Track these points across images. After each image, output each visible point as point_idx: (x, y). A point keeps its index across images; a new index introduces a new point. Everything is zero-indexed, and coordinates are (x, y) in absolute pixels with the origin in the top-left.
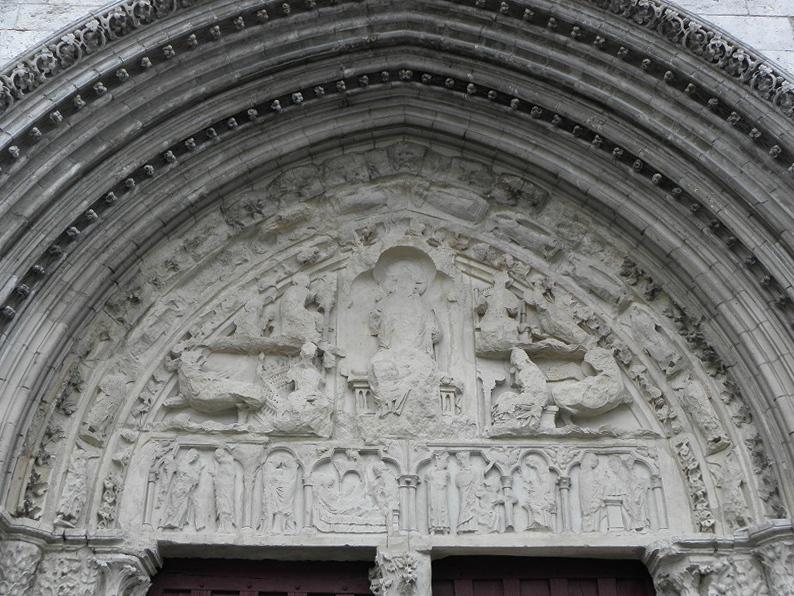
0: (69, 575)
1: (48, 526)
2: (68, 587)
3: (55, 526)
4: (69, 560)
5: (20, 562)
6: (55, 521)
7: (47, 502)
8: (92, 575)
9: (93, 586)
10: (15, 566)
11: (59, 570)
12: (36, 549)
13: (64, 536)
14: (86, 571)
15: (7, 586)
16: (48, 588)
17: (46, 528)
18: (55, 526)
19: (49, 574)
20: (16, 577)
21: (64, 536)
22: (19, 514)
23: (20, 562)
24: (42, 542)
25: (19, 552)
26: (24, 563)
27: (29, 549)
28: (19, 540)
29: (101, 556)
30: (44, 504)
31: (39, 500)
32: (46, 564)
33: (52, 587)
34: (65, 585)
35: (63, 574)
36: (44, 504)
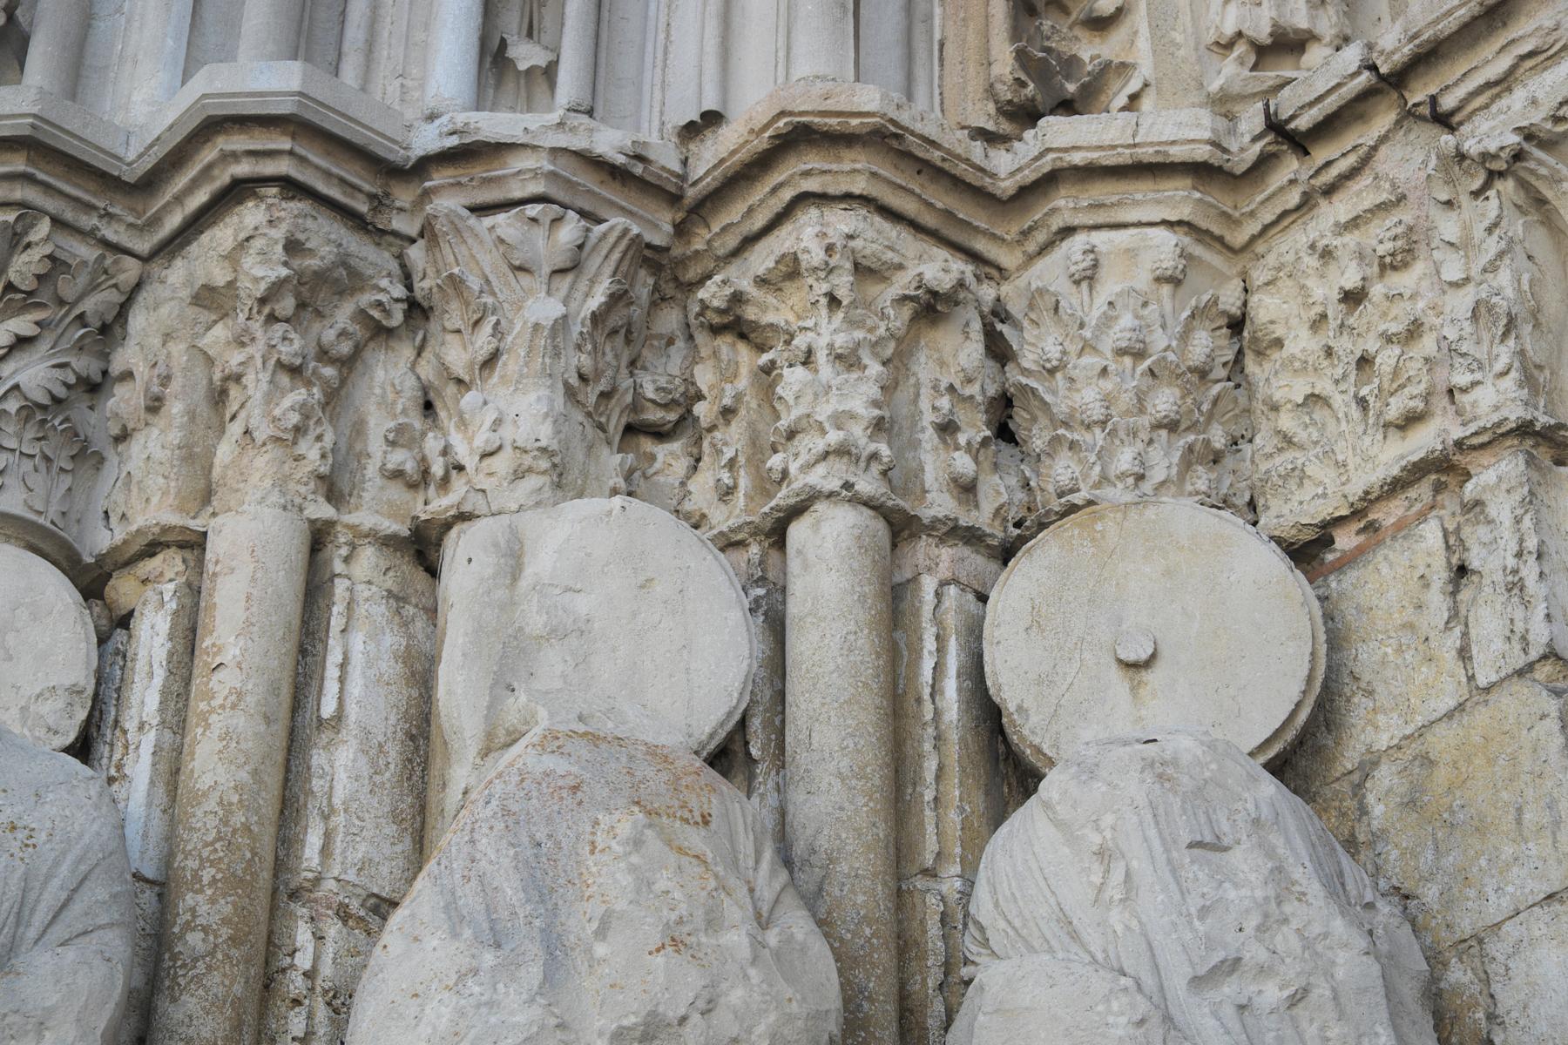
0: (1377, 290)
1: (1185, 115)
2: (1388, 339)
3: (1224, 104)
4: (1354, 223)
5: (1107, 321)
6: (1214, 86)
7: (1154, 28)
8: (1479, 232)
9: (1504, 278)
10: (1087, 347)
11: (1324, 291)
12: (1164, 247)
13: (1275, 127)
14: (1449, 227)
15: (1073, 445)
16: (1314, 399)
17: (1177, 127)
18: (1224, 104)
19: (1301, 342)
20: (1108, 400)
21: (1275, 127)
22: (1026, 115)
23: (1107, 321)
24: (1179, 199)
25: (1088, 277)
26: (1126, 320)
27: (1131, 253)
28: (1068, 231)
29: (1482, 124)
30: (1143, 44)
31: (1118, 36)
32: (1267, 309)
33: (1324, 386)
34: (1372, 344)
35: (1353, 298)
36: (1143, 44)
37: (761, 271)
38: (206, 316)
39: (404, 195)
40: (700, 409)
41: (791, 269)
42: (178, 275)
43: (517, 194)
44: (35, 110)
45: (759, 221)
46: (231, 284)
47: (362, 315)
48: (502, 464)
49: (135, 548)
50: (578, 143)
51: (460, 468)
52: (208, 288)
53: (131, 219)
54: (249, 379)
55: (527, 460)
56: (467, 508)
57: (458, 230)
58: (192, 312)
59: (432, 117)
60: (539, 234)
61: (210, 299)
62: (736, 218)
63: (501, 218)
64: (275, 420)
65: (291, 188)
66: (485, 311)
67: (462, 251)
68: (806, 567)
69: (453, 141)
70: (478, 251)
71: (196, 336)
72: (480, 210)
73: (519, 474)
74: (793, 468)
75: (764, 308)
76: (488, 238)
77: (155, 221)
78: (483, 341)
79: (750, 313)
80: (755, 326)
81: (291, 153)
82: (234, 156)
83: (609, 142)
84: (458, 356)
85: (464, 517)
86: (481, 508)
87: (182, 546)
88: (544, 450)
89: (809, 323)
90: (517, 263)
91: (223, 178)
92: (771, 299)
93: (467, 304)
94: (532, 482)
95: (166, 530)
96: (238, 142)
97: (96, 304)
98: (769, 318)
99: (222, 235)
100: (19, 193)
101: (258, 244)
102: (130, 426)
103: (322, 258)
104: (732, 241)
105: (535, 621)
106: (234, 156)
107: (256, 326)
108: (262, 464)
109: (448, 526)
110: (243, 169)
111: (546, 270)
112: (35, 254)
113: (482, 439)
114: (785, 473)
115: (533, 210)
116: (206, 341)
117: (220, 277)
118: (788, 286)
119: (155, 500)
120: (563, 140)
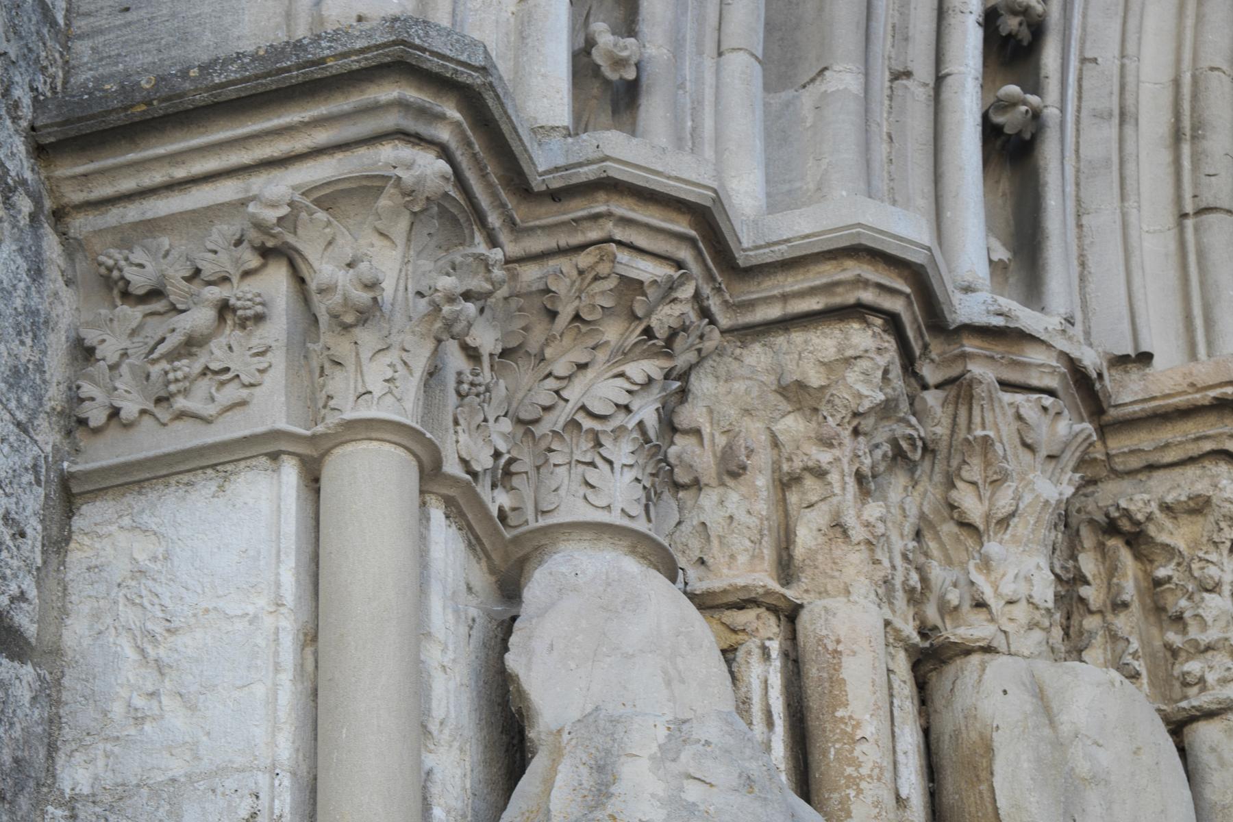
37: (1169, 499)
38: (784, 406)
39: (937, 348)
40: (1084, 591)
41: (1199, 506)
42: (757, 356)
43: (1035, 382)
44: (715, 185)
45: (1170, 457)
46: (822, 388)
47: (894, 442)
48: (1021, 612)
49: (732, 598)
50: (1075, 354)
51: (980, 605)
52: (801, 385)
53: (727, 296)
54: (834, 477)
55: (1037, 616)
56: (995, 644)
57: (991, 399)
58: (774, 398)
59: (968, 289)
60: (1046, 420)
61: (797, 394)
62: (1146, 446)
63: (1019, 398)
64: (868, 525)
65: (893, 323)
66: (1004, 477)
67: (989, 416)
68: (1222, 763)
69: (999, 322)
70: (997, 419)
71: (773, 420)
72: (1006, 385)
73: (1032, 626)
74: (1211, 678)
75: (1161, 528)
76: (1011, 412)
77: (751, 305)
78: (1004, 501)
79: (1152, 530)
80: (1150, 541)
81: (908, 296)
82: (866, 284)
83: (1090, 359)
84: (972, 505)
85: (988, 649)
86: (1003, 648)
87: (774, 610)
88: (1048, 610)
89: (1213, 557)
90: (1029, 441)
91: (851, 298)
92: (1168, 524)
93: (988, 464)
94: (1038, 635)
95: (769, 593)
96: (870, 272)
97: (683, 359)
98: (1163, 538)
99: (823, 342)
100: (685, 254)
101: (865, 364)
102: (704, 480)
103: (894, 389)
104: (1135, 463)
105: (1083, 768)
106: (866, 284)
107: (846, 433)
108: (855, 559)
109: (968, 652)
110: (868, 296)
111: (1043, 453)
112: (677, 309)
113: (1008, 589)
114: (1202, 680)
115: (1048, 401)
116: (778, 427)
117: (815, 378)
118: (1184, 519)
119: (742, 559)
120: (1061, 344)
